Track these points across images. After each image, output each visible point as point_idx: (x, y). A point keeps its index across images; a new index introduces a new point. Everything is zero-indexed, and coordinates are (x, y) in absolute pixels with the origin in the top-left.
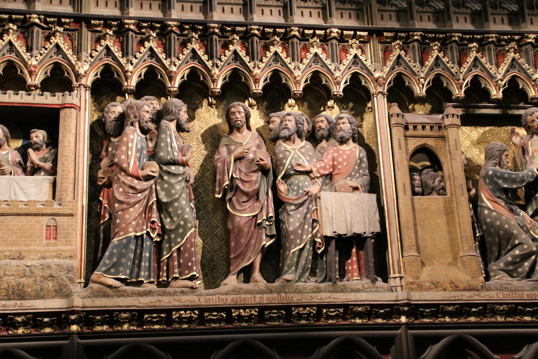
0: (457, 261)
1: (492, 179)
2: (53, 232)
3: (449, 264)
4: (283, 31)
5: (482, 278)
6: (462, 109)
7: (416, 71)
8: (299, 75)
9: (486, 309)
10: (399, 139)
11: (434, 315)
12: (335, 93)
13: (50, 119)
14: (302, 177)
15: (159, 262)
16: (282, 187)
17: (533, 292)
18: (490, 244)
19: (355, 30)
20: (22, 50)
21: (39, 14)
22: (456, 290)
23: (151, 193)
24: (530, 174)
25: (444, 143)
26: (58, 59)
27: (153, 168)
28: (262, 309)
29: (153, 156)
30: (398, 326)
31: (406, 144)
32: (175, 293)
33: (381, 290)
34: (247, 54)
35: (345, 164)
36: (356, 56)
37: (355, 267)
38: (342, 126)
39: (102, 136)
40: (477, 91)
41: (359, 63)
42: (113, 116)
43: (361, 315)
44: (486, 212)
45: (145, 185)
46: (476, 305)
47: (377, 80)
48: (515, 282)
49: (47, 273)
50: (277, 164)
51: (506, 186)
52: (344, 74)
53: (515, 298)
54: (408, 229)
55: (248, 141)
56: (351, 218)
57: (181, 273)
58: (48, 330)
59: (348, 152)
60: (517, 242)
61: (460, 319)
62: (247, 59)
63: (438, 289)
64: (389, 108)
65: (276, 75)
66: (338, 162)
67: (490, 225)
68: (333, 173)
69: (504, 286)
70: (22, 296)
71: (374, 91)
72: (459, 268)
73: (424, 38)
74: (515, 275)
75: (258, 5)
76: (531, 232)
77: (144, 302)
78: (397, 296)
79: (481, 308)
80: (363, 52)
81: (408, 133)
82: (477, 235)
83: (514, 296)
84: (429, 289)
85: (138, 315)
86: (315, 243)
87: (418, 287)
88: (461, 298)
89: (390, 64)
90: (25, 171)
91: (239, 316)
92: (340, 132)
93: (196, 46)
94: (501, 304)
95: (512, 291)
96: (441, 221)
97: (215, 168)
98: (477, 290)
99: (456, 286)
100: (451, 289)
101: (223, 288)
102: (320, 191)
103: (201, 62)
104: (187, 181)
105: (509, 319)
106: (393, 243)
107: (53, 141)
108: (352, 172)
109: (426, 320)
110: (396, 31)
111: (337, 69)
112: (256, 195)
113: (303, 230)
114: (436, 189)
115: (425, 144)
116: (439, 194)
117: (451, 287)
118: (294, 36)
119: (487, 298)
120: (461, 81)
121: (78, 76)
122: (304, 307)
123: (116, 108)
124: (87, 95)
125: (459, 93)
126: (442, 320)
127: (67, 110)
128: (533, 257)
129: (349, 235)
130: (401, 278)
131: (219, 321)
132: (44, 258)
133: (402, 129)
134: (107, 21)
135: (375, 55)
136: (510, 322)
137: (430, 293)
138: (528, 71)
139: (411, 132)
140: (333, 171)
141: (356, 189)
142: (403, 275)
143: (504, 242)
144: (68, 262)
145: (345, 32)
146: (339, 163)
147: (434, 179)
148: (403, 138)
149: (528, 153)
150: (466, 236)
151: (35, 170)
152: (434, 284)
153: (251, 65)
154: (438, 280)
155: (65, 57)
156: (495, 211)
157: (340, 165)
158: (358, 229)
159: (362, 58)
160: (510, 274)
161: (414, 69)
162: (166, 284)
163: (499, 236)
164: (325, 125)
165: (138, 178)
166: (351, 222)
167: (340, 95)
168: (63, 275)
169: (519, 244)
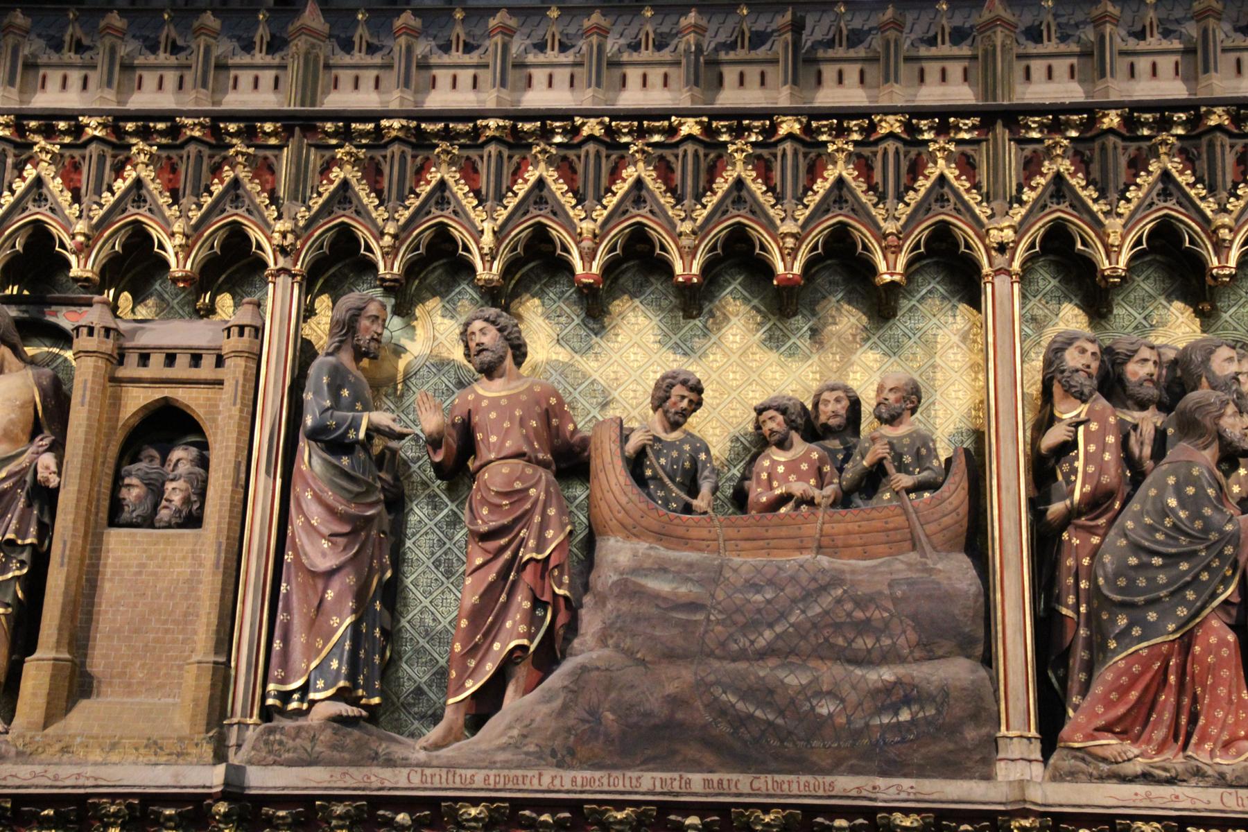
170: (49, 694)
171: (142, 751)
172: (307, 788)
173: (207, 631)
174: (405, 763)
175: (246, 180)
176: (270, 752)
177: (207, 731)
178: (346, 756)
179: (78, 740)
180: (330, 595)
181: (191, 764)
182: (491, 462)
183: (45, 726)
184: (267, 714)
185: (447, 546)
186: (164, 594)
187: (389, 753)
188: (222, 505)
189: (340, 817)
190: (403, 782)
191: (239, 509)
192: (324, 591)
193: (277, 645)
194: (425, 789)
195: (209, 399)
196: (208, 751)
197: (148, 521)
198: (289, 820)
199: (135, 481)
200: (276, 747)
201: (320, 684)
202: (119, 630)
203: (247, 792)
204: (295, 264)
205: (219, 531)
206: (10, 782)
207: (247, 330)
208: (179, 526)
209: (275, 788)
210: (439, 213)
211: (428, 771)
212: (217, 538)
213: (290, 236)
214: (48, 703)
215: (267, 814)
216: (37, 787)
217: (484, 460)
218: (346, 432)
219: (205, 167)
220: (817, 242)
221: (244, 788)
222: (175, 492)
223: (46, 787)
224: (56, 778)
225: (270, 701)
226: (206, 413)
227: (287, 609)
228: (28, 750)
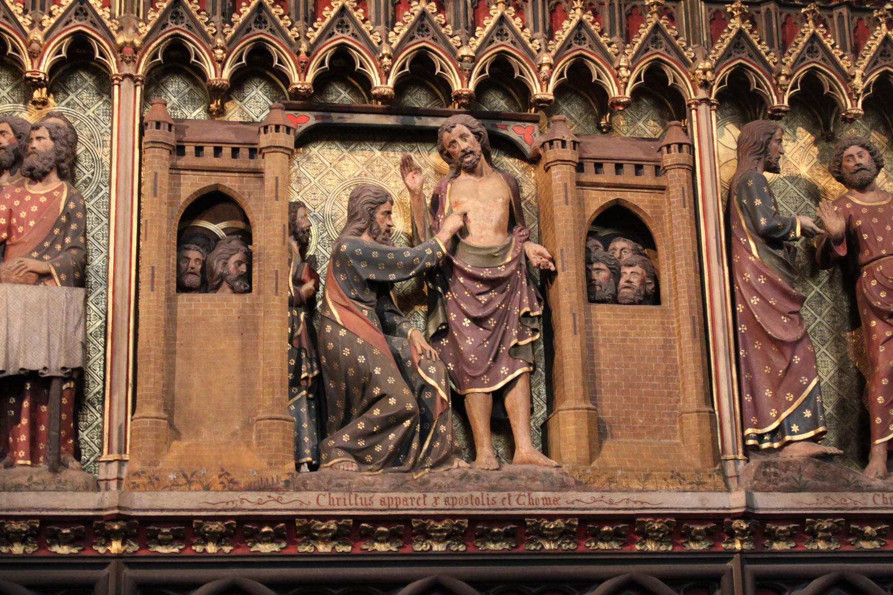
0: (251, 430)
5: (292, 465)
6: (316, 113)
7: (210, 33)
10: (156, 174)
12: (28, 75)
17: (394, 495)
18: (327, 394)
22: (230, 490)
24: (429, 252)
25: (259, 184)
30: (103, 562)
31: (175, 186)
33: (68, 487)
35: (32, 223)
37: (23, 438)
38: (35, 144)
41: (90, 12)
44: (329, 329)
46: (271, 520)
47: (121, 49)
51: (373, 276)
52: (51, 36)
53: (354, 506)
54: (149, 362)
56: (20, 338)
59: (43, 200)
60: (377, 391)
61: (238, 547)
63: (192, 488)
66: (18, 218)
67: (334, 356)
68: (8, 243)
69: (334, 482)
71: (117, 72)
72: (248, 444)
74: (369, 458)
76: (420, 371)
78: (102, 501)
79: (282, 525)
81: (182, 162)
82: (303, 376)
83: (353, 501)
84: (174, 486)
87: (151, 483)
88: (239, 505)
92: (31, 156)
94: (325, 519)
95: (349, 491)
96: (229, 346)
98: (277, 490)
99: (232, 481)
100: (220, 487)
105: (341, 549)
106: (115, 389)
108: (45, 241)
114: (229, 277)
115: (217, 185)
116: (234, 290)
117: (222, 483)
119: (296, 505)
120: (303, 55)
125: (301, 81)
126: (199, 549)
128: (407, 423)
129: (11, 371)
130: (121, 462)
133: (165, 154)
136: (344, 554)
137: (174, 494)
138: (451, 40)
139: (189, 159)
140: (8, 238)
141: (44, 276)
142: (126, 457)
143: (356, 391)
146: (21, 222)
147: (228, 259)
149: (443, 209)
150: (272, 378)
152: (185, 476)
154: (195, 468)
156: (344, 328)
157: (22, 225)
158: (35, 361)
160: (358, 456)
161: (206, 29)
164: (9, 141)
166: (18, 347)
167: (40, 79)
169: (382, 396)
170: (589, 436)
171: (669, 481)
172: (801, 509)
173: (697, 387)
174: (870, 489)
175: (665, 25)
176: (769, 481)
177: (715, 466)
178: (827, 484)
179: (619, 472)
180: (797, 359)
181: (710, 491)
182: (883, 256)
183: (591, 462)
184: (748, 451)
185: (818, 320)
186: (646, 357)
187: (857, 481)
188: (688, 287)
189: (826, 531)
190: (870, 504)
191: (700, 291)
192: (792, 357)
193: (748, 398)
194: (887, 508)
195: (652, 201)
196: (718, 479)
197: (615, 300)
198: (788, 533)
199: (603, 266)
200: (773, 477)
201: (795, 428)
202: (617, 386)
203: (757, 512)
204: (710, 96)
205: (691, 307)
206: (576, 505)
207: (685, 147)
208: (640, 303)
209: (777, 509)
210: (811, 60)
211: (887, 495)
212: (691, 313)
213: (709, 74)
214: (590, 443)
215: (770, 529)
216: (598, 509)
217: (875, 255)
218: (789, 233)
219: (623, 14)
220: (724, 78)
221: (754, 509)
222: (632, 276)
223: (604, 509)
224: (611, 502)
225: (750, 442)
226: (652, 213)
227: (749, 370)
228: (584, 481)
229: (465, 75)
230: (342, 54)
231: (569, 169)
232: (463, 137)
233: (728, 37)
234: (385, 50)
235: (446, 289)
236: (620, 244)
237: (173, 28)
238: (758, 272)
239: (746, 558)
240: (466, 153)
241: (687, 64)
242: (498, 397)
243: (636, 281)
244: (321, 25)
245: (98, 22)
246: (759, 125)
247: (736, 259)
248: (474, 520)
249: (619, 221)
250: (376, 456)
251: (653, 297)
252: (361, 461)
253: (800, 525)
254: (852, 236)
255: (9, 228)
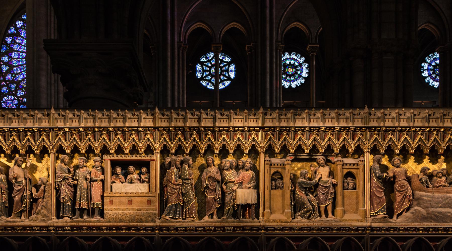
1: (300, 184)
2: (149, 202)
3: (281, 214)
4: (227, 129)
8: (232, 146)
9: (291, 229)
11: (273, 230)
13: (147, 164)
14: (231, 184)
15: (183, 212)
16: (224, 187)
18: (296, 206)
19: (254, 127)
20: (137, 141)
21: (142, 127)
23: (180, 190)
26: (149, 143)
27: (180, 181)
28: (215, 227)
29: (180, 177)
30: (261, 233)
31: (270, 171)
32: (187, 222)
34: (214, 139)
36: (254, 138)
39: (164, 169)
40: (300, 149)
42: (167, 163)
43: (248, 230)
45: (178, 187)
47: (261, 147)
48: (303, 220)
49: (148, 215)
50: (223, 179)
55: (213, 170)
57: (189, 216)
58: (150, 232)
62: (213, 141)
64: (265, 156)
65: (224, 146)
67: (298, 200)
70: (142, 222)
73: (281, 130)
75: (219, 118)
77: (178, 224)
80: (257, 135)
81: (271, 167)
85: (176, 229)
86: (234, 206)
89: (266, 141)
90: (140, 181)
91: (208, 229)
93: (195, 136)
96: (280, 199)
97: (202, 180)
101: (203, 221)
102: (237, 188)
103: (197, 142)
104: (192, 185)
107: (148, 172)
109: (270, 232)
110: (270, 127)
111: (246, 143)
112: (214, 190)
113: (230, 202)
118: (231, 131)
121: (155, 149)
122: (229, 227)
123: (168, 160)
124: (158, 156)
125: (292, 151)
127: (152, 162)
131: (202, 230)
132: (147, 210)
134: (164, 129)
135: (262, 137)
139: (273, 166)
141: (250, 188)
143: (302, 206)
144: (155, 212)
145: (250, 129)
146: (245, 178)
148: (269, 169)
151: (143, 182)
153: (214, 143)
155: (151, 142)
159: (256, 139)
162: (185, 219)
163: (300, 204)
165: (175, 185)
168: (153, 216)
184: (371, 216)
229: (322, 148)
230: (300, 146)
231: (341, 166)
232: (322, 160)
233: (373, 139)
234: (308, 145)
235: (317, 188)
236: (349, 179)
237: (270, 142)
238: (376, 184)
239: (369, 234)
240: (322, 163)
241: (365, 145)
242: (326, 207)
243: (352, 186)
244: (296, 141)
245: (257, 142)
246: (377, 156)
247: (372, 181)
248: (322, 227)
249: (350, 175)
250: (305, 217)
251: (355, 189)
252: (302, 218)
253: (380, 229)
254: (394, 177)
255: (243, 179)
